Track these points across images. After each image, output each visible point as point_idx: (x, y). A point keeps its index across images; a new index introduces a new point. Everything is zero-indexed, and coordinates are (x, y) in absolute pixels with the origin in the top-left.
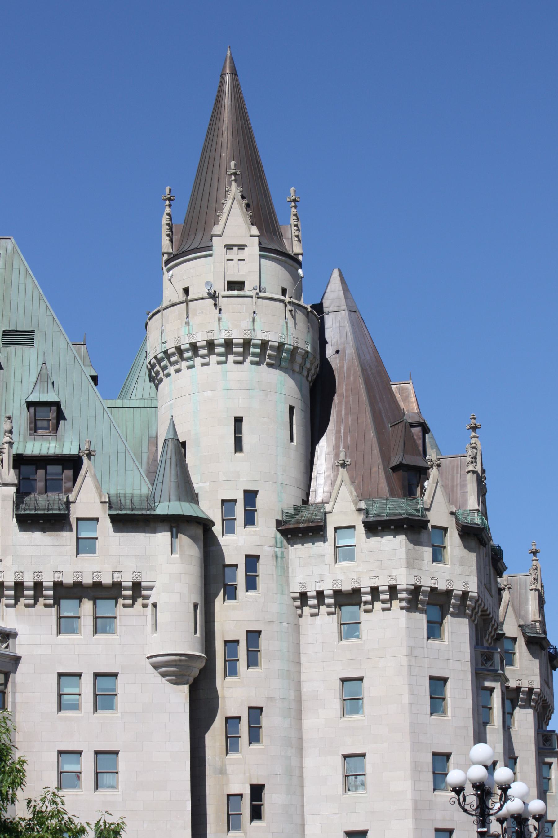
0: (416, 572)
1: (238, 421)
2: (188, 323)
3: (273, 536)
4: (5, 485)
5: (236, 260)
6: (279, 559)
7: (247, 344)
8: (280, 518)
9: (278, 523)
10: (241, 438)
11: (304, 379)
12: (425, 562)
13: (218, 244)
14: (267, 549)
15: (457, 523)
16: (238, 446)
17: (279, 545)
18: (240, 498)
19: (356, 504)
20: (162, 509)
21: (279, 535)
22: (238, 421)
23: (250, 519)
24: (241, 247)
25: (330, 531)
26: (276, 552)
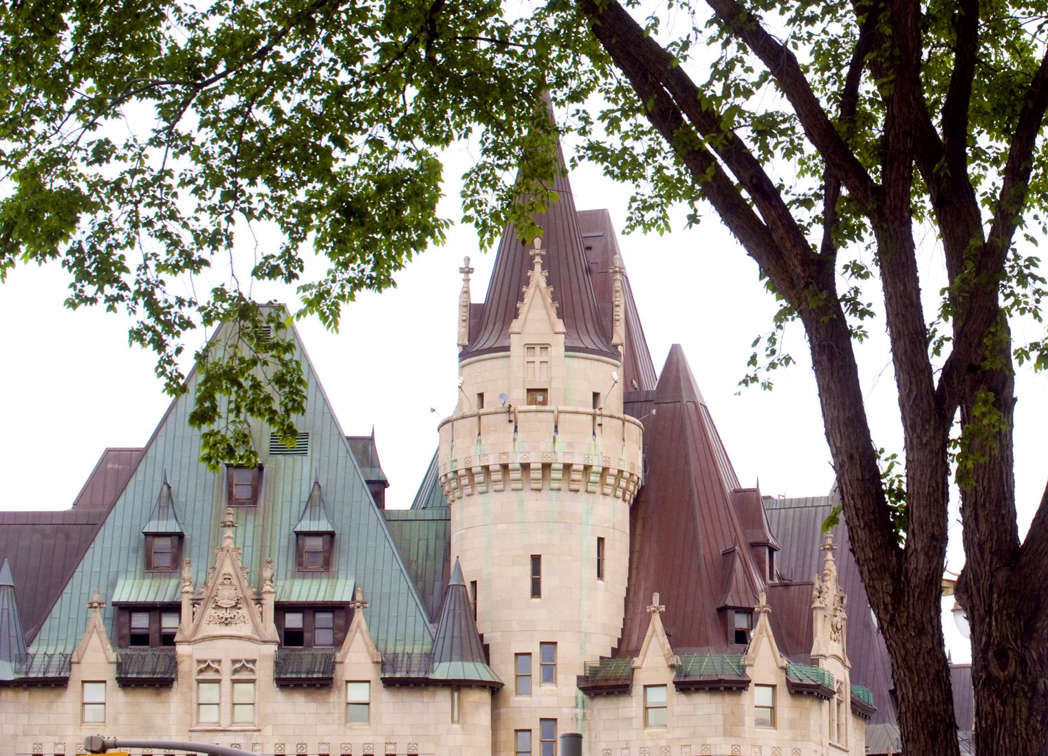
0: (733, 741)
1: (536, 560)
2: (479, 441)
3: (574, 695)
4: (265, 642)
5: (537, 363)
6: (580, 722)
7: (546, 467)
8: (582, 674)
9: (579, 678)
10: (539, 579)
11: (620, 500)
12: (746, 728)
13: (516, 343)
14: (566, 710)
15: (788, 681)
16: (536, 591)
17: (580, 705)
18: (535, 649)
19: (667, 660)
20: (442, 671)
21: (580, 693)
22: (536, 560)
23: (549, 673)
24: (545, 347)
25: (637, 689)
26: (576, 714)
